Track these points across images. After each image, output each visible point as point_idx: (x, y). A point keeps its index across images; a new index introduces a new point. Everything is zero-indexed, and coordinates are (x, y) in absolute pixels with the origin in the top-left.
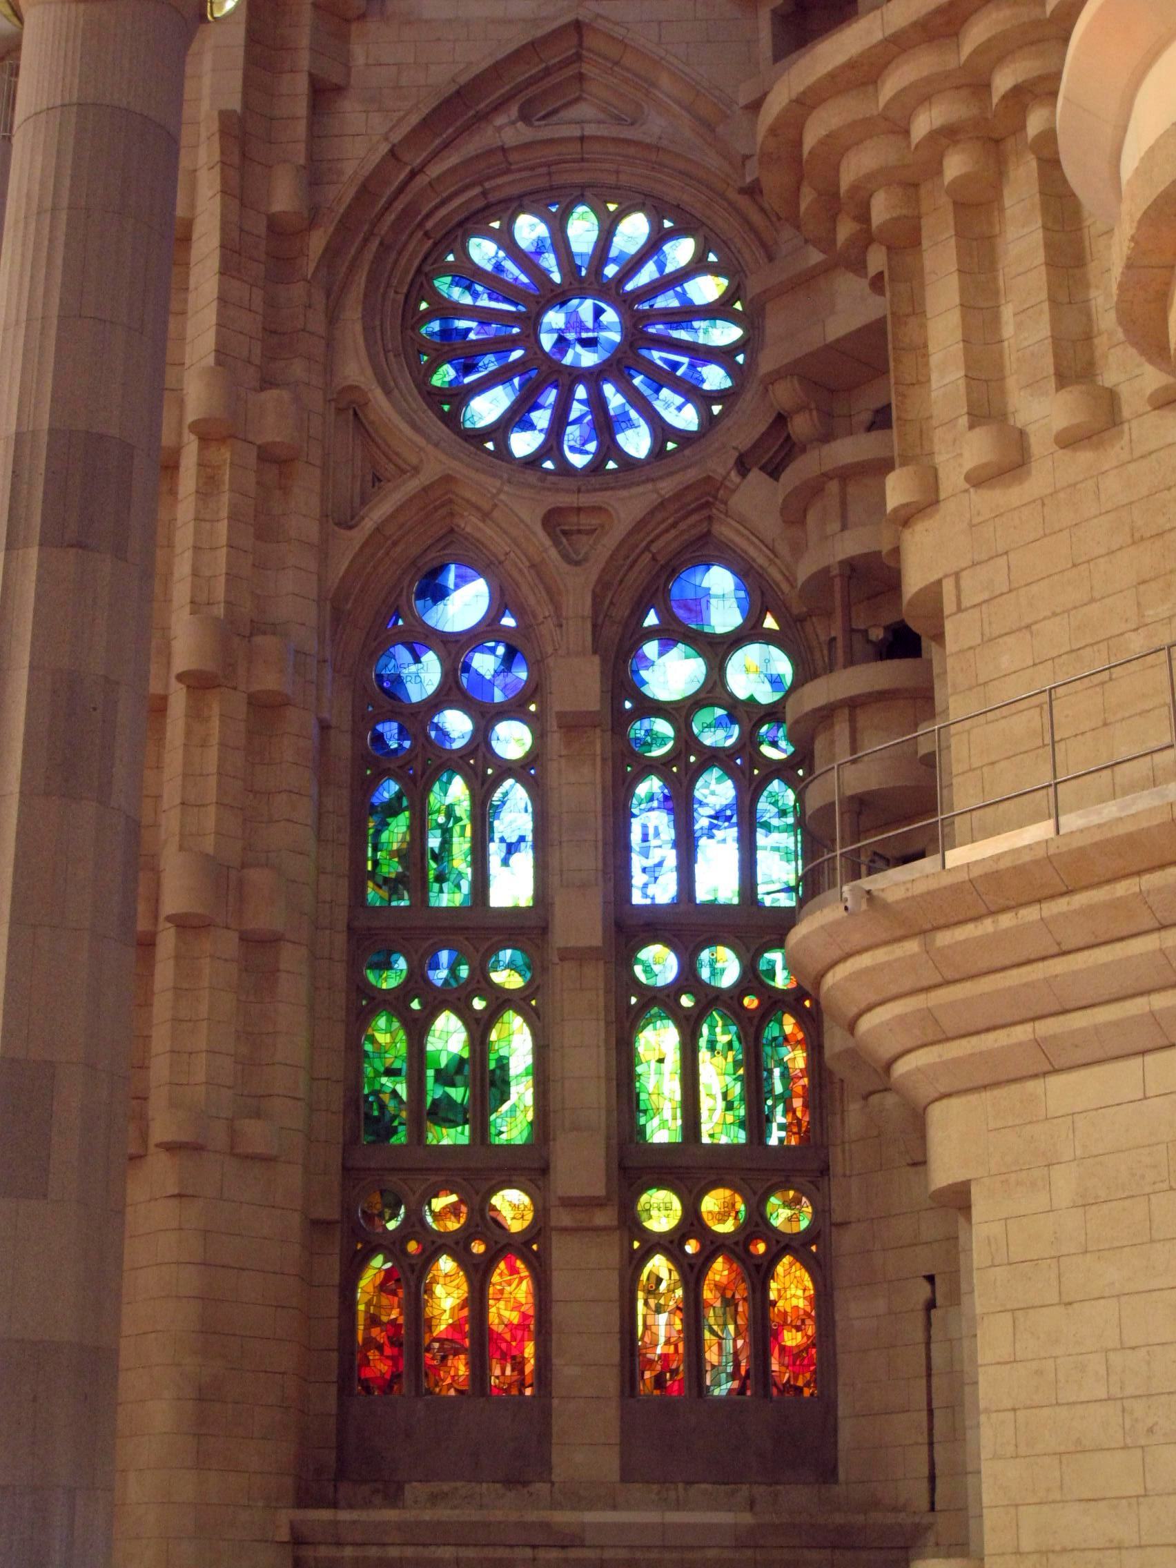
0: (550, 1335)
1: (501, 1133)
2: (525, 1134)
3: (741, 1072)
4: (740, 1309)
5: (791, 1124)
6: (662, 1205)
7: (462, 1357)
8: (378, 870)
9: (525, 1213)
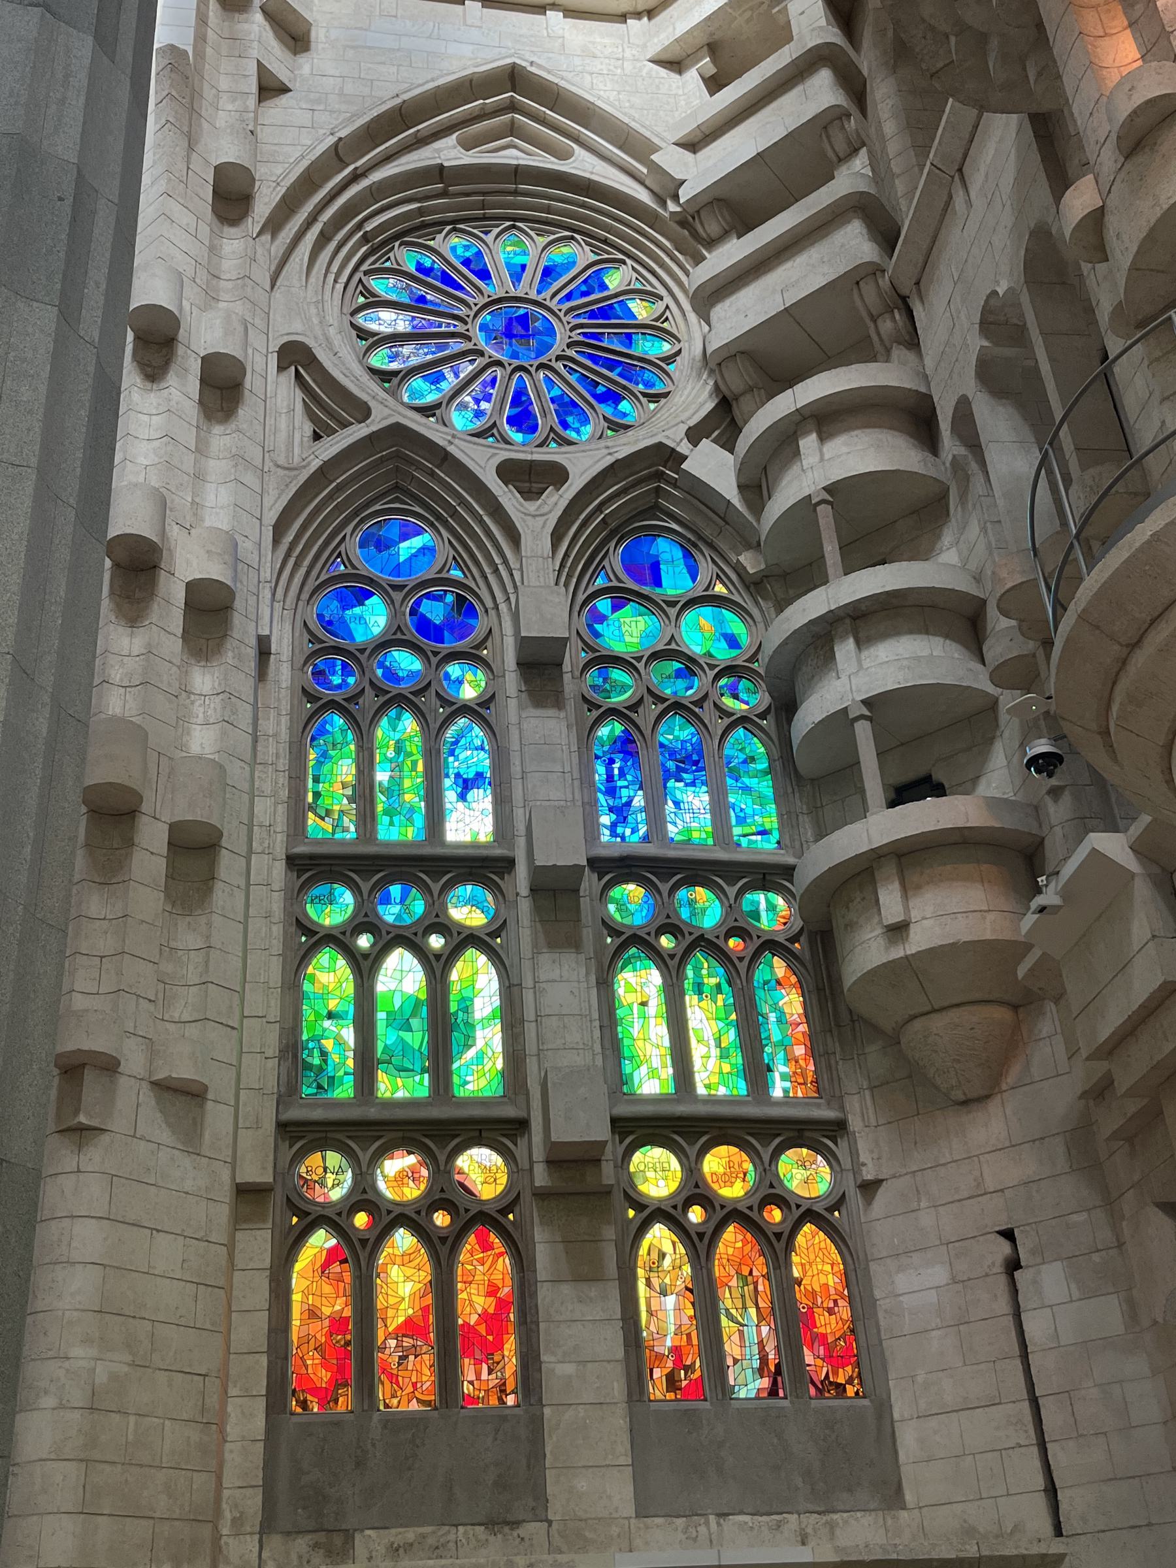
1: (466, 1083)
2: (494, 1084)
3: (734, 1016)
4: (760, 1288)
9: (498, 1175)
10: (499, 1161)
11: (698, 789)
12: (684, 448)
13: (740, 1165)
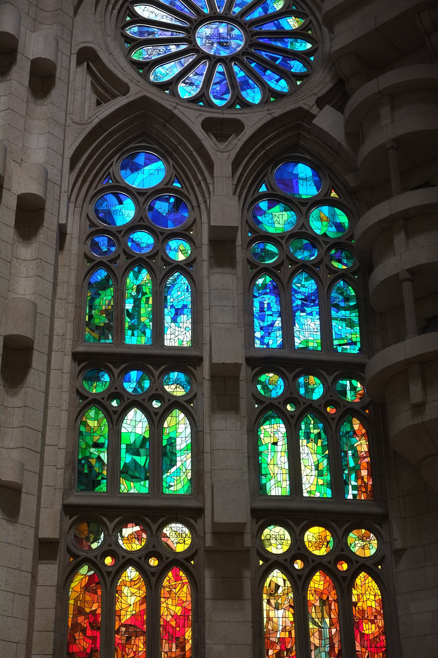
0: (204, 622)
2: (186, 488)
3: (327, 452)
4: (333, 607)
5: (361, 486)
6: (278, 536)
7: (142, 638)
8: (92, 321)
10: (187, 531)
11: (313, 317)
12: (314, 110)
13: (325, 538)
